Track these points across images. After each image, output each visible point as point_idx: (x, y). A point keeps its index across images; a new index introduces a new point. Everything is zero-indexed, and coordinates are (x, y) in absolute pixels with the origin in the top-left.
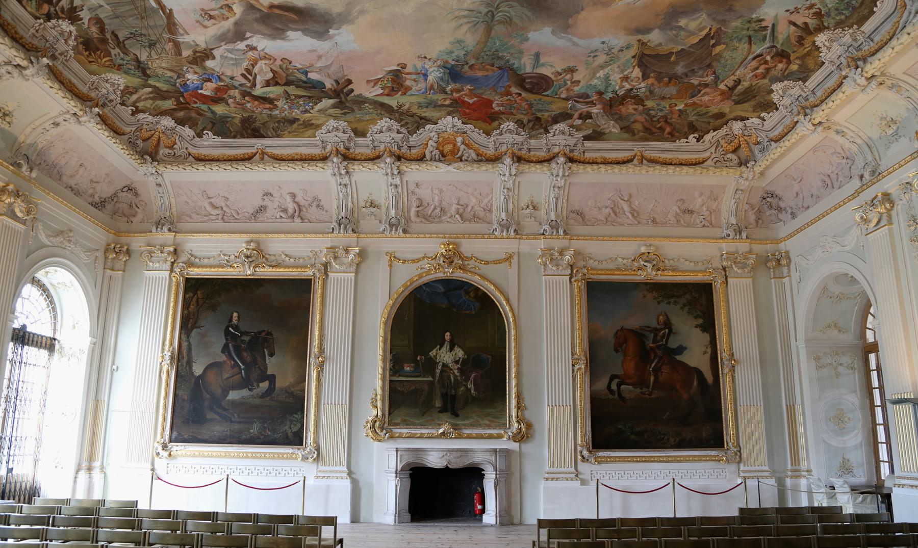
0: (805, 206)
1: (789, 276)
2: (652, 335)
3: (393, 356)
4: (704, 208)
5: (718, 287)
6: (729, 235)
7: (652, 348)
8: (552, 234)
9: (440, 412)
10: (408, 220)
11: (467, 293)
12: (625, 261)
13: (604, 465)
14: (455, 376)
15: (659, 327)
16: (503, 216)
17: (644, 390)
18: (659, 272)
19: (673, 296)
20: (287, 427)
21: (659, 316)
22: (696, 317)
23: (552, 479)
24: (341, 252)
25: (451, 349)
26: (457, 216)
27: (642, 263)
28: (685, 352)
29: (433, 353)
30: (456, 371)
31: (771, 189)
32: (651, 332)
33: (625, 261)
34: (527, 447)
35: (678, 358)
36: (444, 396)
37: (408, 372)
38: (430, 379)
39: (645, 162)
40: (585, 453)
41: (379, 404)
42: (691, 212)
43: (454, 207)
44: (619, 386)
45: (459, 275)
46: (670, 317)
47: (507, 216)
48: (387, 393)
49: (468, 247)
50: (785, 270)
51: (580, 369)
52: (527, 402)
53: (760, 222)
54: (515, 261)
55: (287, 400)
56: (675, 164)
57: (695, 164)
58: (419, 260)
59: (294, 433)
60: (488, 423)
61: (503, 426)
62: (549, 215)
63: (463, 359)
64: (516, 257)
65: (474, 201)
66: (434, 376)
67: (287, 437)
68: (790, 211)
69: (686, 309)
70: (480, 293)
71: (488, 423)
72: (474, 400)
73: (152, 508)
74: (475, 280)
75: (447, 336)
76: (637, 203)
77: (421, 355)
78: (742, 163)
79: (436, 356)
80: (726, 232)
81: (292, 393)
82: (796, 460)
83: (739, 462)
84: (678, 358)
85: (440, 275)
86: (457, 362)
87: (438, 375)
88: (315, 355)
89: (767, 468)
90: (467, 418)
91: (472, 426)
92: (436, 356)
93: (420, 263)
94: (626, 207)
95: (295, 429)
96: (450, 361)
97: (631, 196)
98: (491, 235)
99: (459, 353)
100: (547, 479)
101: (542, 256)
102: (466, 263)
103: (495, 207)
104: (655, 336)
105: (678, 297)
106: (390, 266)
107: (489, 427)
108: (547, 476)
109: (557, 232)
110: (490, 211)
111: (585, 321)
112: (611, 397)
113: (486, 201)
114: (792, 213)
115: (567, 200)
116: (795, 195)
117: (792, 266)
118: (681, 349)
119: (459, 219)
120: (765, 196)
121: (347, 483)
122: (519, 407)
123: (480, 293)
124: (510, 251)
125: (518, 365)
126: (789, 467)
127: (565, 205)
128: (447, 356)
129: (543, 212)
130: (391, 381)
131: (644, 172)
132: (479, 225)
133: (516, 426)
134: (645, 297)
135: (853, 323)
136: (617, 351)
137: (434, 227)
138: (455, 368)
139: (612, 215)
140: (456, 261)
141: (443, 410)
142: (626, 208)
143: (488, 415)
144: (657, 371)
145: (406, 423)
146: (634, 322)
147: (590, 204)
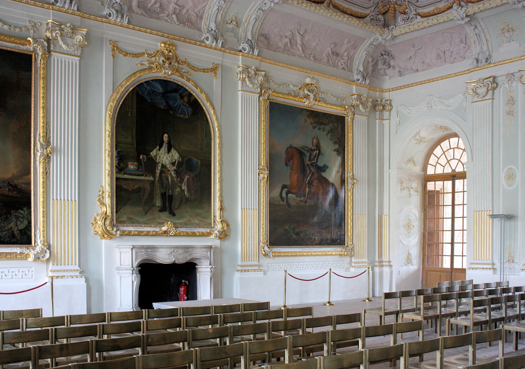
0: (415, 69)
1: (390, 119)
2: (308, 155)
3: (118, 153)
4: (346, 54)
5: (348, 120)
6: (358, 80)
7: (308, 165)
8: (248, 53)
9: (161, 211)
10: (130, 9)
11: (182, 97)
12: (295, 88)
13: (276, 258)
14: (172, 177)
15: (313, 148)
16: (213, 26)
17: (302, 198)
18: (317, 103)
19: (322, 124)
20: (12, 224)
21: (313, 139)
22: (335, 143)
23: (245, 271)
24: (68, 30)
25: (169, 151)
26: (174, 16)
27: (306, 92)
28: (327, 170)
29: (153, 153)
30: (173, 173)
31: (389, 49)
32: (308, 151)
33: (295, 88)
34: (227, 244)
35: (323, 174)
36: (163, 195)
37: (131, 170)
38: (151, 178)
39: (331, 6)
40: (266, 248)
41: (108, 201)
42: (337, 55)
43: (172, 6)
44: (287, 194)
45: (176, 78)
46: (320, 140)
47: (216, 27)
48: (115, 191)
49: (187, 52)
50: (386, 114)
51: (264, 178)
52: (225, 205)
53: (374, 73)
54: (219, 72)
55: (11, 194)
56: (348, 14)
57: (359, 18)
58: (141, 55)
59: (21, 231)
60: (197, 222)
61: (209, 225)
62: (246, 34)
63: (179, 162)
64: (220, 69)
65: (191, 4)
66: (154, 177)
67: (13, 235)
68: (398, 69)
69: (330, 135)
70: (192, 99)
71: (197, 222)
72: (188, 200)
73: (55, 316)
74: (189, 86)
75: (166, 137)
76: (307, 38)
77: (143, 154)
78: (386, 25)
79: (156, 156)
80: (356, 77)
81: (15, 186)
82: (380, 255)
83: (351, 257)
84: (323, 174)
85: (161, 74)
86: (173, 164)
87: (158, 175)
88: (41, 145)
89: (366, 260)
90: (181, 217)
91: (185, 225)
92: (156, 156)
93: (141, 59)
94: (299, 42)
95: (22, 227)
96: (167, 163)
97: (306, 31)
98: (201, 43)
99: (175, 155)
100: (242, 271)
101: (243, 72)
102: (181, 66)
103: (205, 16)
104: (310, 156)
105: (326, 125)
106: (113, 56)
107: (199, 226)
108: (239, 268)
109: (253, 52)
110: (201, 18)
111: (268, 136)
112: (281, 203)
113: (200, 7)
114: (399, 71)
115: (261, 24)
116: (409, 57)
117: (394, 112)
118: (324, 168)
119: (175, 19)
120: (383, 53)
121: (82, 281)
122: (221, 209)
123: (192, 99)
124: (216, 62)
125: (221, 171)
126: (377, 259)
127: (259, 27)
128: (165, 157)
129: (241, 30)
130: (117, 179)
131: (329, 15)
132: (191, 30)
133: (219, 226)
134: (305, 121)
135: (420, 159)
136: (287, 165)
137: (154, 22)
138: (172, 169)
139: (289, 45)
140: (173, 64)
141: (163, 209)
142: (299, 42)
143: (197, 215)
144: (310, 183)
145: (132, 222)
146: (298, 142)
147: (276, 31)
